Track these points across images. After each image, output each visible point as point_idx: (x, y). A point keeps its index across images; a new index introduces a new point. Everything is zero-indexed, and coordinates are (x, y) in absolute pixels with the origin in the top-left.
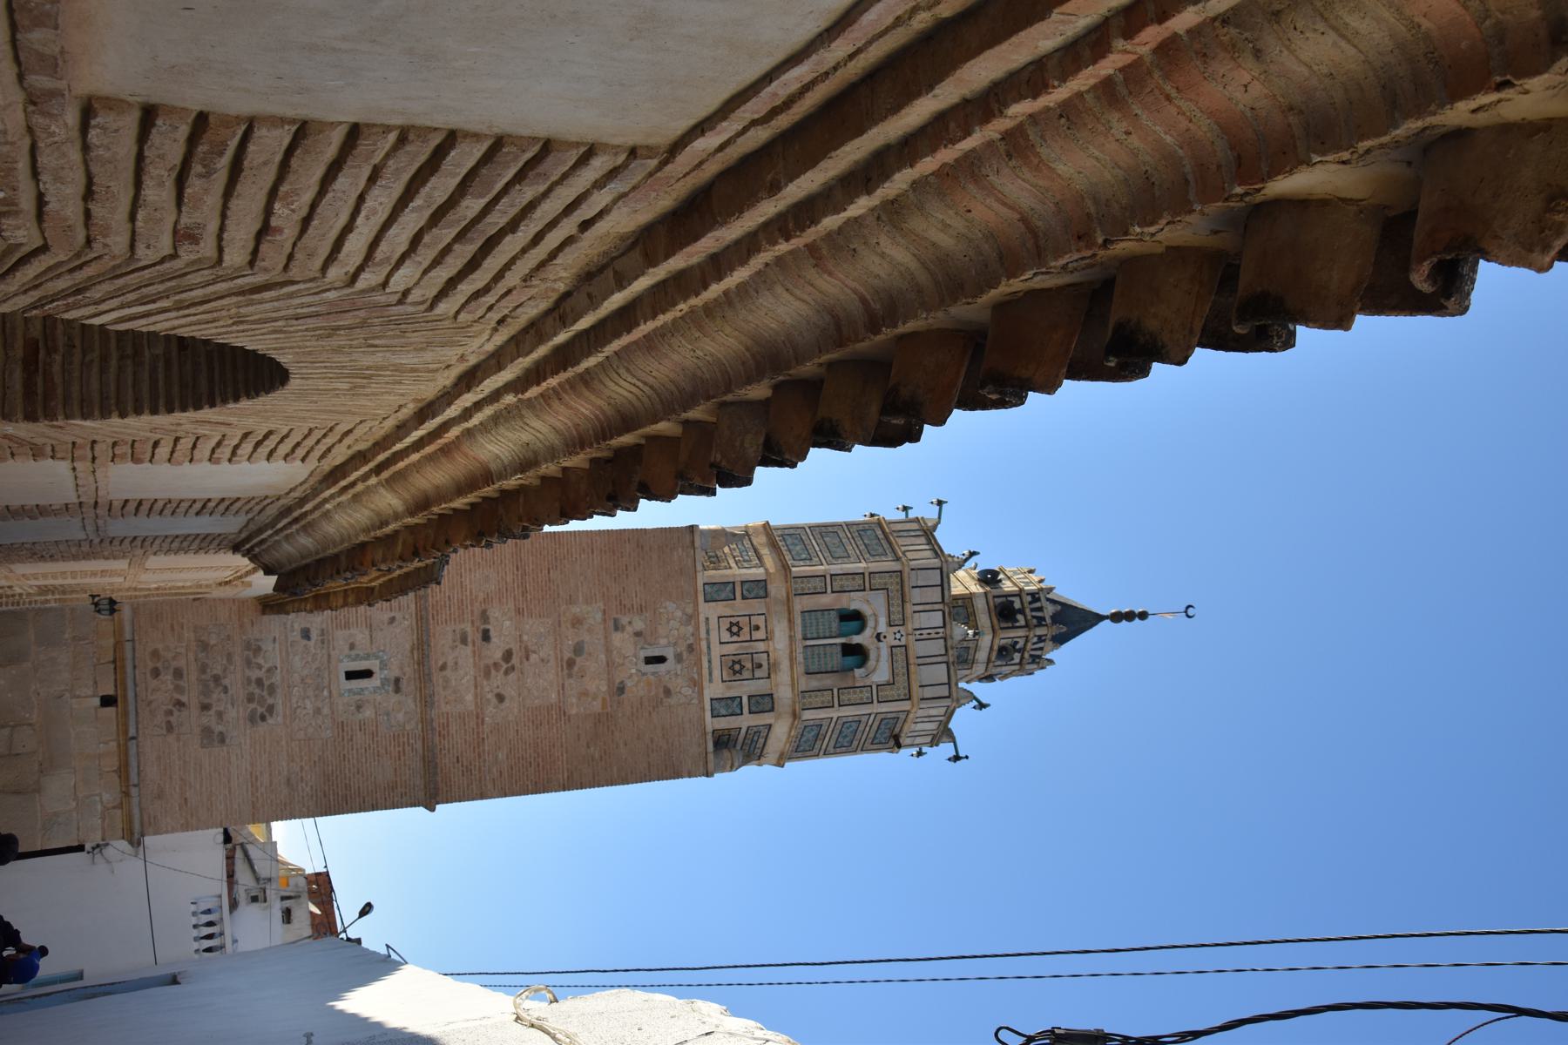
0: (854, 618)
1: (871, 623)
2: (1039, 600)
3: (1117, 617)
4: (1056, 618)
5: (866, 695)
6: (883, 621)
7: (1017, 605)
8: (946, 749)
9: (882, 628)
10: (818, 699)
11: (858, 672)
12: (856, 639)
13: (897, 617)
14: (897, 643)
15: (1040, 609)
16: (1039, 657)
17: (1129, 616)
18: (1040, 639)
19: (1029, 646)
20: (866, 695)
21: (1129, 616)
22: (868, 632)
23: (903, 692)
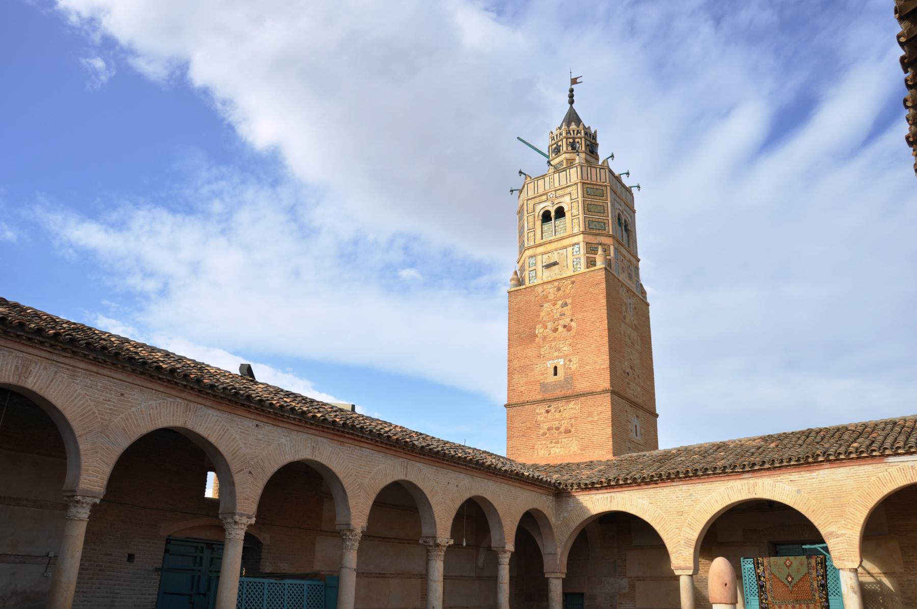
1: (547, 209)
9: (548, 203)
12: (553, 214)
13: (544, 198)
17: (571, 97)
21: (571, 97)
23: (575, 187)
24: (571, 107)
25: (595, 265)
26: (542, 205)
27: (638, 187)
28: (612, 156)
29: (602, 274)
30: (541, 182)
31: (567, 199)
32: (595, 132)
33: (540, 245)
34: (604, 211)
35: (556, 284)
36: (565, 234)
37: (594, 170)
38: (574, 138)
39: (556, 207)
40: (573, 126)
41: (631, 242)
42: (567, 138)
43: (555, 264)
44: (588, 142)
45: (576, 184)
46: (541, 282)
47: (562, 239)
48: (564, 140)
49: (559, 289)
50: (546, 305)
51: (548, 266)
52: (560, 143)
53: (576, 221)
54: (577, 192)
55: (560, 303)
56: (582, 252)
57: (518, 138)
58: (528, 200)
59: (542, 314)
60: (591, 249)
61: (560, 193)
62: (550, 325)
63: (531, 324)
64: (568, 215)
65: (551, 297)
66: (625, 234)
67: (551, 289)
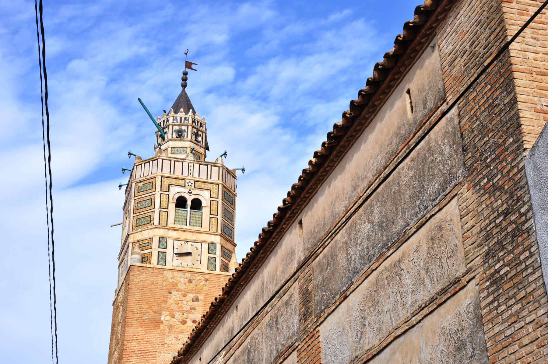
0: (181, 203)
1: (183, 194)
2: (176, 117)
4: (187, 112)
5: (214, 203)
6: (182, 189)
7: (177, 128)
8: (238, 173)
12: (189, 203)
13: (182, 183)
14: (193, 185)
15: (181, 118)
16: (201, 123)
17: (185, 80)
18: (194, 121)
19: (196, 127)
20: (214, 203)
21: (185, 80)
22: (187, 196)
24: (184, 91)
25: (228, 271)
30: (178, 165)
31: (206, 194)
33: (174, 229)
35: (188, 275)
36: (202, 229)
39: (194, 197)
42: (193, 127)
43: (189, 254)
46: (173, 268)
48: (190, 128)
49: (190, 281)
50: (174, 293)
51: (181, 255)
52: (184, 128)
53: (213, 220)
55: (191, 296)
57: (139, 99)
59: (170, 301)
62: (178, 315)
63: (156, 308)
64: (205, 211)
65: (181, 286)
67: (182, 279)
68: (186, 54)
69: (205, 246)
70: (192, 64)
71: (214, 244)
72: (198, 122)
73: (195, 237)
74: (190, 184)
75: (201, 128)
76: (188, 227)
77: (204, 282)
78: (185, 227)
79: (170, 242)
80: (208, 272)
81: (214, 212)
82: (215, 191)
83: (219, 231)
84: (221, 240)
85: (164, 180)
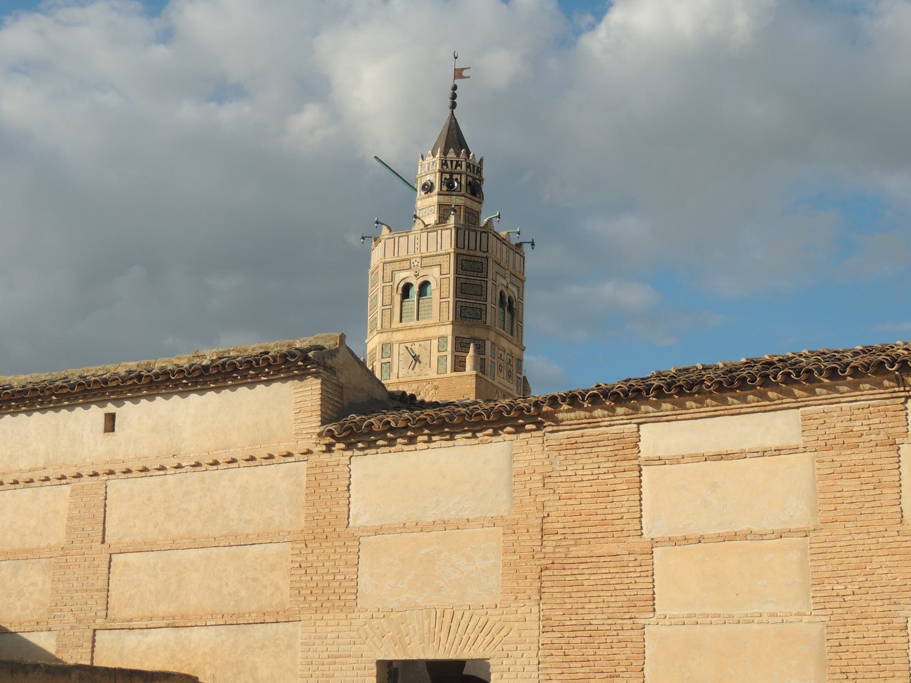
1: (408, 280)
3: (454, 106)
10: (445, 309)
11: (433, 286)
13: (406, 264)
16: (457, 162)
17: (454, 96)
21: (454, 96)
22: (413, 280)
23: (446, 258)
26: (403, 275)
27: (533, 244)
28: (499, 217)
29: (473, 381)
30: (403, 240)
32: (481, 160)
33: (398, 330)
34: (481, 292)
36: (430, 322)
37: (472, 234)
38: (451, 174)
40: (451, 155)
41: (515, 325)
44: (470, 179)
45: (449, 254)
46: (396, 380)
47: (426, 326)
53: (444, 305)
54: (449, 264)
56: (449, 349)
58: (385, 263)
60: (460, 345)
61: (426, 261)
66: (507, 315)
68: (456, 58)
69: (435, 343)
70: (463, 70)
71: (445, 337)
72: (452, 162)
73: (421, 334)
74: (416, 264)
75: (459, 168)
76: (414, 323)
77: (433, 391)
78: (412, 323)
79: (396, 346)
80: (436, 376)
81: (443, 295)
82: (445, 265)
83: (451, 319)
84: (453, 330)
85: (387, 266)
